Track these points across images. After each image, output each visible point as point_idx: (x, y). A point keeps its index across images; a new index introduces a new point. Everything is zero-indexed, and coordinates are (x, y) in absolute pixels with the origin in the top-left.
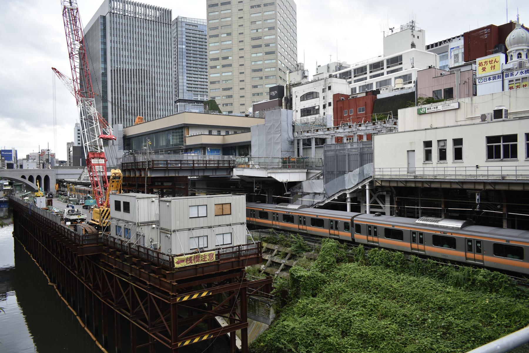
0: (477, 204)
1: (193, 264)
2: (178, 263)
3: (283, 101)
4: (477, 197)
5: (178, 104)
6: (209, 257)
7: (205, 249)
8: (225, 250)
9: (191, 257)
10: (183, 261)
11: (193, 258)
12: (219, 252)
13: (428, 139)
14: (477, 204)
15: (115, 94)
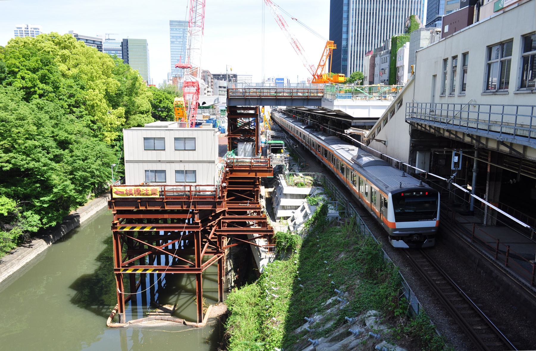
0: (454, 171)
1: (134, 197)
2: (116, 193)
3: (475, 8)
4: (455, 159)
5: (436, 23)
6: (153, 191)
7: (151, 184)
8: (175, 187)
9: (130, 190)
10: (122, 193)
11: (133, 192)
12: (165, 189)
13: (453, 55)
14: (454, 171)
15: (358, 18)
